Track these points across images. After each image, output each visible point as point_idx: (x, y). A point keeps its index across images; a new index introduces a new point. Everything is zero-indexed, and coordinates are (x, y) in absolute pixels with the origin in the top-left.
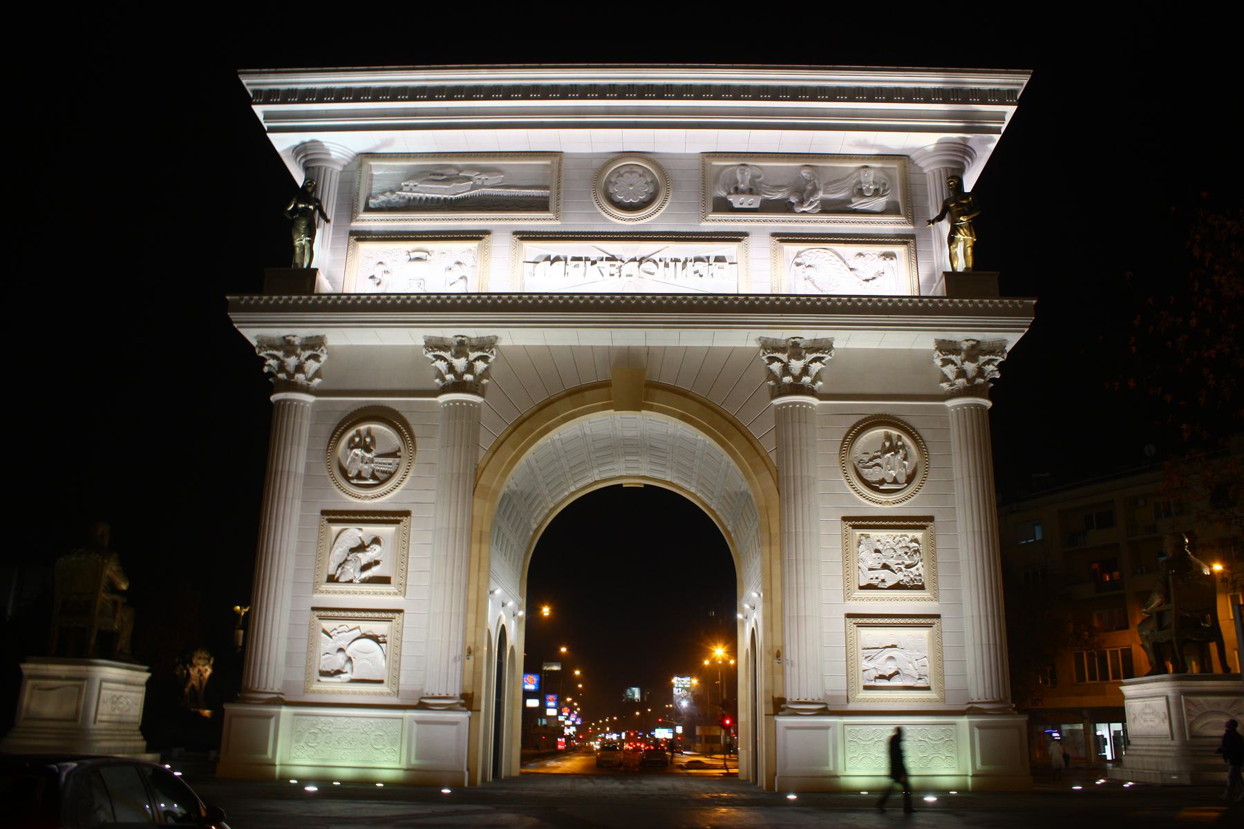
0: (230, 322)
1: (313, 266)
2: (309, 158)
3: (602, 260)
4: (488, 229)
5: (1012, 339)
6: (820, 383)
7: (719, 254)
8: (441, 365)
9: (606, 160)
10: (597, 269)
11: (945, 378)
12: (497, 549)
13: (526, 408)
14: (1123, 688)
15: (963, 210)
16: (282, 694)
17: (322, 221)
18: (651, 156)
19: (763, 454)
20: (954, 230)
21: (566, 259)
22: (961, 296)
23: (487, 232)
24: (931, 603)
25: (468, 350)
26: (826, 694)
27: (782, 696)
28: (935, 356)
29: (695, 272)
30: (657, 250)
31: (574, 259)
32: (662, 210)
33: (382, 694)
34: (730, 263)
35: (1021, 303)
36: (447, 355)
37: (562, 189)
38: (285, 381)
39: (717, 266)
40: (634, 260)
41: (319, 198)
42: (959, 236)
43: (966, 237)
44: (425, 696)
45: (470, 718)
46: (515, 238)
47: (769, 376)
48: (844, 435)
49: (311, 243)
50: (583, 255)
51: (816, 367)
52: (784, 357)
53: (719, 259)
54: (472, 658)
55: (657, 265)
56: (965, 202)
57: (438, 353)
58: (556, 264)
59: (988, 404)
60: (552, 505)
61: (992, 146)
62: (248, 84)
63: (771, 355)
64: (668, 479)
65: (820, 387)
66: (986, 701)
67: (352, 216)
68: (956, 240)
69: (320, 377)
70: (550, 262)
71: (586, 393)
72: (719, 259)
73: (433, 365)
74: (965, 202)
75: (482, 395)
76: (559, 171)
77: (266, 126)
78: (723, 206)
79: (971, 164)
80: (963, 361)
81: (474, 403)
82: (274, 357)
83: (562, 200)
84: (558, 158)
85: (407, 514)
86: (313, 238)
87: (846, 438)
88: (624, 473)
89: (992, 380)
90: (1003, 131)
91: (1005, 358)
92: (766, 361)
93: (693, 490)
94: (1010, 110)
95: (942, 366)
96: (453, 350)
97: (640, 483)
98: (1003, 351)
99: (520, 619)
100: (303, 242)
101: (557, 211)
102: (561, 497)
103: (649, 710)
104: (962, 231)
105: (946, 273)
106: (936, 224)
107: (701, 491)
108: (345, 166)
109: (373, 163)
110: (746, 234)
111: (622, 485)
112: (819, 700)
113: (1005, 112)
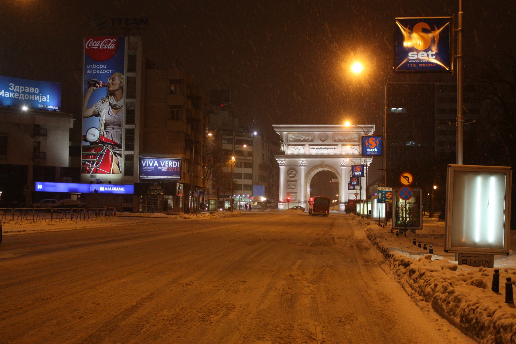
0: (275, 159)
3: (320, 148)
8: (301, 163)
13: (311, 168)
31: (317, 148)
52: (342, 162)
53: (335, 148)
67: (288, 142)
72: (335, 148)
76: (314, 135)
78: (335, 141)
85: (297, 181)
97: (327, 170)
101: (314, 142)
109: (290, 134)
110: (338, 145)
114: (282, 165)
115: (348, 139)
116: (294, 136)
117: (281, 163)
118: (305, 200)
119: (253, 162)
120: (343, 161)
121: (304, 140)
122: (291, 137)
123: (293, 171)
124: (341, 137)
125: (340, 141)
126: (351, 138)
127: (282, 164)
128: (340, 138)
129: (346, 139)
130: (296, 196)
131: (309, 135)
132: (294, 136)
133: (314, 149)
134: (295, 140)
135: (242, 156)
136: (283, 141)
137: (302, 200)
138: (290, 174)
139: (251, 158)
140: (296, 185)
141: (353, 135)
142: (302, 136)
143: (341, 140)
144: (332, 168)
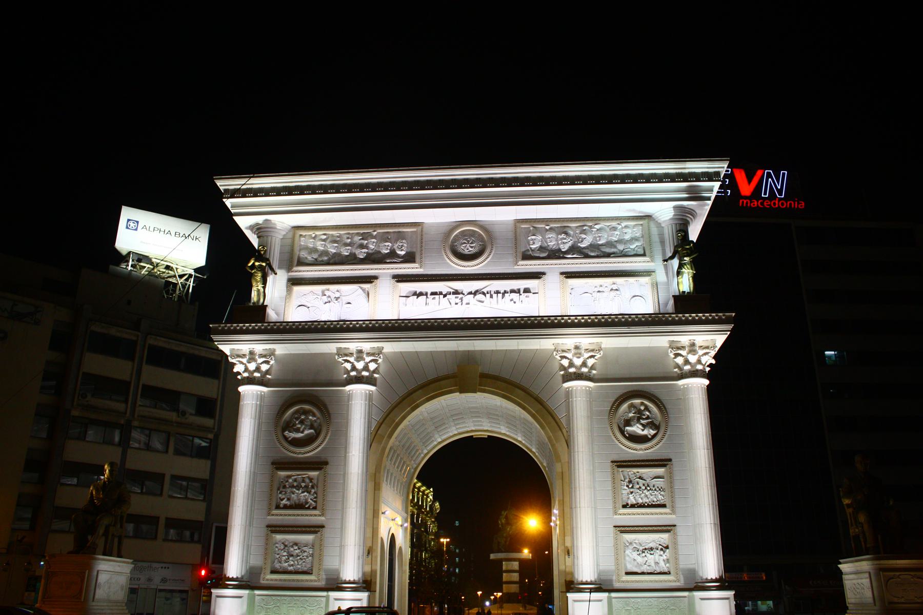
1: (265, 304)
2: (262, 230)
3: (450, 294)
4: (376, 275)
5: (720, 340)
6: (594, 372)
7: (526, 286)
8: (348, 366)
9: (451, 227)
10: (447, 300)
11: (677, 366)
12: (387, 484)
13: (402, 392)
14: (840, 566)
15: (687, 253)
16: (249, 582)
17: (270, 272)
18: (481, 223)
19: (558, 420)
20: (681, 266)
21: (426, 294)
22: (684, 312)
23: (376, 278)
24: (670, 516)
25: (365, 356)
26: (600, 579)
27: (571, 580)
28: (669, 352)
29: (512, 300)
30: (487, 285)
31: (433, 294)
32: (488, 260)
33: (311, 581)
34: (533, 293)
35: (724, 315)
36: (352, 359)
37: (423, 248)
38: (248, 377)
39: (525, 296)
40: (470, 293)
41: (268, 257)
42: (684, 270)
43: (688, 270)
44: (339, 582)
45: (369, 596)
46: (393, 281)
47: (560, 368)
48: (611, 404)
49: (264, 288)
50: (438, 290)
51: (590, 362)
53: (527, 291)
54: (370, 556)
55: (485, 296)
56: (688, 247)
57: (345, 358)
58: (420, 297)
59: (707, 382)
60: (425, 451)
61: (708, 208)
62: (220, 186)
63: (561, 355)
64: (503, 432)
65: (594, 375)
66: (702, 581)
68: (681, 273)
69: (270, 375)
70: (416, 297)
71: (443, 383)
72: (527, 291)
73: (343, 365)
74: (688, 247)
75: (374, 385)
76: (422, 235)
77: (232, 211)
78: (527, 257)
79: (693, 220)
80: (688, 354)
81: (370, 391)
82: (241, 363)
83: (424, 255)
84: (420, 227)
85: (326, 463)
86: (266, 285)
87: (612, 407)
88: (474, 429)
89: (709, 366)
90: (713, 199)
91: (717, 351)
92: (560, 359)
93: (520, 439)
94: (716, 185)
95: (674, 358)
96: (355, 356)
97: (485, 435)
98: (715, 347)
99: (406, 528)
100: (259, 288)
102: (432, 445)
103: (479, 593)
104: (685, 267)
105: (674, 296)
106: (669, 261)
107: (524, 440)
108: (284, 235)
109: (304, 233)
110: (544, 274)
111: (472, 436)
112: (596, 581)
113: (713, 186)
114: (250, 381)
115: (593, 246)
116: (324, 240)
117: (246, 370)
118: (368, 569)
119: (217, 436)
120: (577, 348)
121: (375, 258)
122: (306, 248)
123: (306, 412)
124: (557, 240)
125: (555, 254)
126: (610, 244)
127: (252, 373)
128: (552, 244)
129: (581, 246)
130: (318, 549)
131: (394, 232)
132: (324, 240)
133: (423, 298)
134: (326, 258)
135: (177, 410)
136: (266, 260)
137: (351, 571)
138: (289, 426)
139: (208, 422)
140: (320, 485)
141: (614, 229)
142: (362, 239)
143: (559, 250)
144: (517, 389)
